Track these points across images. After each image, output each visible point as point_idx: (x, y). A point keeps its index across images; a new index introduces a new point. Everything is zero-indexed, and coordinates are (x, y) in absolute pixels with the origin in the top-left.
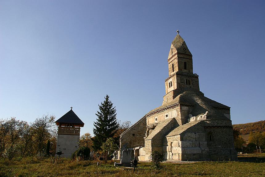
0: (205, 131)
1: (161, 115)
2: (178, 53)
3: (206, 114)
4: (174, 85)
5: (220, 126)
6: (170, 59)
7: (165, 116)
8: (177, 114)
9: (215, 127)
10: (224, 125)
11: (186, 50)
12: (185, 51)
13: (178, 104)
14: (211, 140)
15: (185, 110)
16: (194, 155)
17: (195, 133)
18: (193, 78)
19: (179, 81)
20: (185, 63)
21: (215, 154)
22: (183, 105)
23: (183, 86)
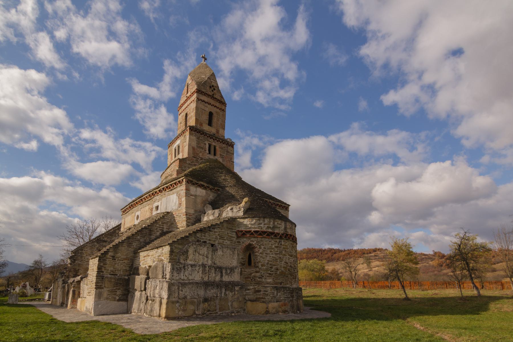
2: (198, 91)
3: (243, 204)
5: (272, 233)
6: (183, 104)
7: (154, 209)
8: (177, 203)
10: (282, 232)
13: (182, 180)
14: (250, 263)
15: (199, 196)
16: (206, 300)
18: (224, 145)
19: (194, 144)
21: (259, 298)
22: (193, 184)
23: (201, 154)
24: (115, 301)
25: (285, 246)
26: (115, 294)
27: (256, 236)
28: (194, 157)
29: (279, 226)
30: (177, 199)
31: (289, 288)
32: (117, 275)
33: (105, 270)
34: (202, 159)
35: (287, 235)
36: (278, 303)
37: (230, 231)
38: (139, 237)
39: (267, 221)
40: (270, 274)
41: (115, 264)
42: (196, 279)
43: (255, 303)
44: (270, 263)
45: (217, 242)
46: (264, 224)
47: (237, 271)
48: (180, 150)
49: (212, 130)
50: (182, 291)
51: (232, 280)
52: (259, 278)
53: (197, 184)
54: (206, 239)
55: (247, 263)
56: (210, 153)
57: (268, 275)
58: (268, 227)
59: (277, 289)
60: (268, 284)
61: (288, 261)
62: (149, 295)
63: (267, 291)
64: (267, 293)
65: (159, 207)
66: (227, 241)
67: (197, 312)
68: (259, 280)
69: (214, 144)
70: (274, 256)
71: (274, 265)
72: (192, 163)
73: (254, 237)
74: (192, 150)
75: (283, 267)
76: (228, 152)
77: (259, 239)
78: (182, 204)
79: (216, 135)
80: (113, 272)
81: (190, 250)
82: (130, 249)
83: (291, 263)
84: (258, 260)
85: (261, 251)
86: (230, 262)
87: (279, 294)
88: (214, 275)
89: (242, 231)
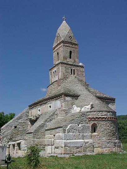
1: (44, 106)
4: (58, 75)
5: (104, 118)
11: (71, 38)
12: (70, 39)
20: (71, 52)
25: (110, 123)
29: (107, 114)
39: (101, 112)
48: (57, 74)
73: (96, 120)
75: (110, 132)
77: (98, 121)
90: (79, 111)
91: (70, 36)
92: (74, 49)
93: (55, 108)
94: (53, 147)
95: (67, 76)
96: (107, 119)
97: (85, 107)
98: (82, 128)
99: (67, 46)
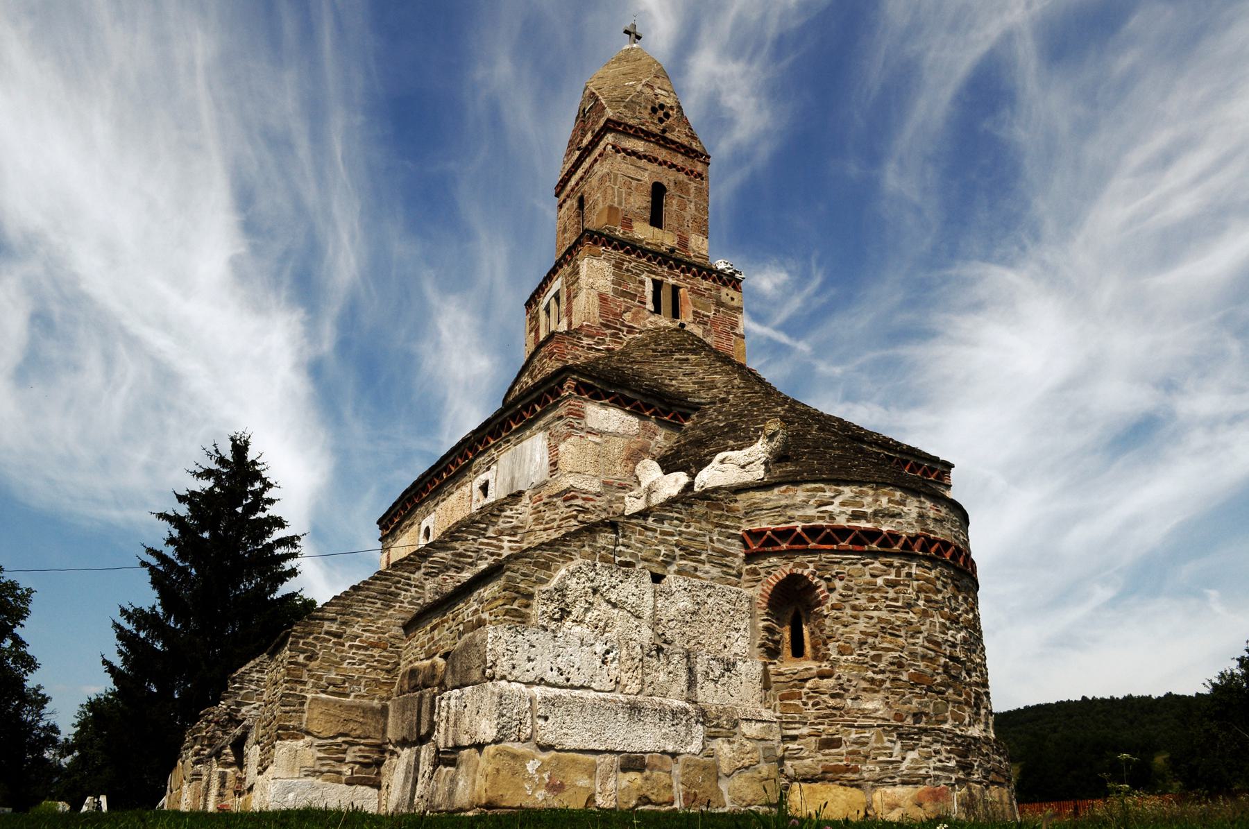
0: (754, 572)
1: (453, 499)
4: (569, 312)
5: (873, 535)
8: (546, 460)
9: (837, 543)
11: (667, 115)
12: (661, 121)
15: (616, 435)
16: (633, 763)
17: (657, 578)
18: (706, 284)
19: (605, 283)
20: (658, 191)
21: (836, 770)
22: (596, 396)
23: (627, 317)
24: (340, 782)
25: (927, 580)
26: (341, 761)
27: (812, 545)
28: (608, 327)
29: (897, 509)
30: (546, 452)
31: (952, 737)
32: (347, 695)
33: (311, 677)
34: (631, 330)
35: (930, 542)
36: (910, 788)
37: (720, 534)
38: (418, 575)
39: (848, 492)
40: (872, 681)
41: (343, 659)
42: (593, 685)
43: (818, 786)
44: (870, 640)
45: (673, 568)
46: (843, 504)
47: (751, 669)
49: (666, 239)
50: (546, 719)
51: (733, 701)
52: (833, 696)
53: (607, 396)
54: (632, 555)
55: (787, 650)
56: (658, 310)
57: (864, 685)
58: (856, 516)
59: (900, 736)
60: (866, 717)
61: (940, 637)
62: (441, 745)
63: (864, 744)
64: (863, 750)
65: (491, 486)
66: (707, 567)
67: (600, 801)
68: (832, 702)
69: (671, 281)
70: (884, 614)
71: (887, 650)
72: (598, 344)
74: (597, 303)
75: (924, 657)
76: (720, 304)
78: (560, 465)
79: (679, 254)
80: (335, 685)
81: (572, 583)
82: (391, 612)
83: (954, 645)
84: (827, 631)
85: (834, 598)
86: (724, 641)
87: (911, 755)
88: (662, 677)
89: (761, 533)
90: (674, 492)
91: (662, 107)
92: (682, 177)
93: (512, 488)
94: (427, 752)
95: (627, 317)
96: (896, 548)
97: (720, 456)
98: (684, 603)
99: (634, 153)
